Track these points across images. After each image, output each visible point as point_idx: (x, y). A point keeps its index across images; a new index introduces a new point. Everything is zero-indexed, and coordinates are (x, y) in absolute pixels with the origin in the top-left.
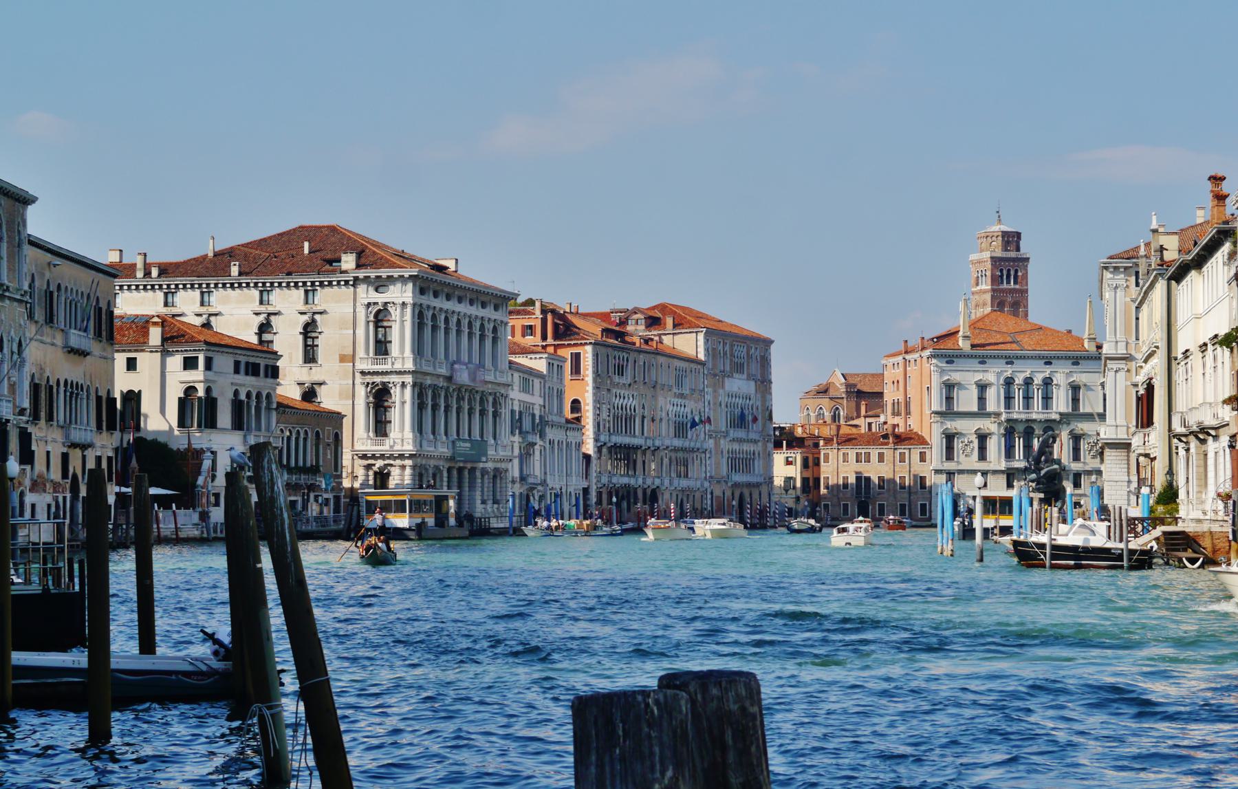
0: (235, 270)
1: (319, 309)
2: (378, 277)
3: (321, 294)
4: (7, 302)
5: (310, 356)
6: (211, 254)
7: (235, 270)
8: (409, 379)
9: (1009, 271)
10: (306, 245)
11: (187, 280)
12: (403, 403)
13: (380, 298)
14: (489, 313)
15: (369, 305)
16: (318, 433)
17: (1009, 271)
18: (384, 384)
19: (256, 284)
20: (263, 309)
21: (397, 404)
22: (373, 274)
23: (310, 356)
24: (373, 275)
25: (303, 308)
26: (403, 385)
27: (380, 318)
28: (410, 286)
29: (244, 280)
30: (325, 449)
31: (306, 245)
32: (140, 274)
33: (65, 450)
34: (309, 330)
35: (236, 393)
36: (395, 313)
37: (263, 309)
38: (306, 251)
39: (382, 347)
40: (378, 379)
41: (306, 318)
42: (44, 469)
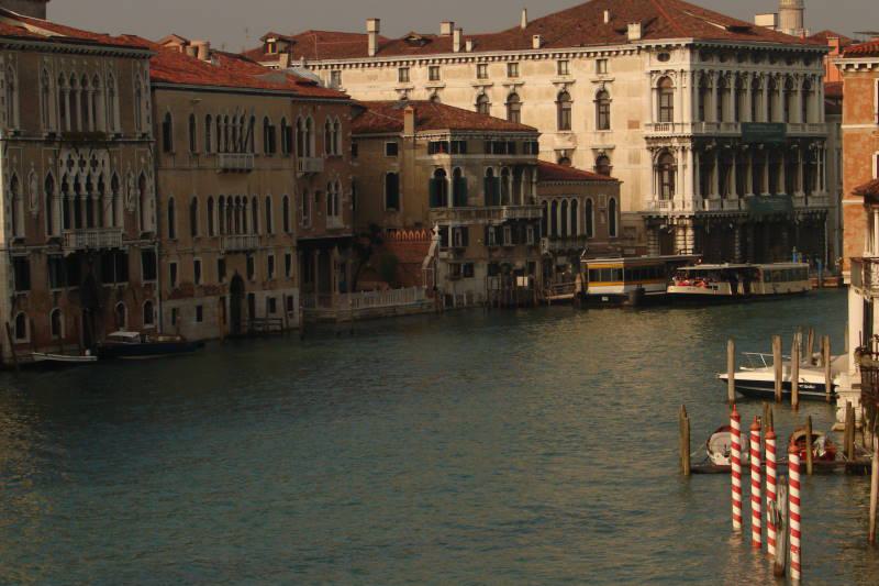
0: (536, 43)
1: (610, 77)
2: (657, 46)
3: (611, 63)
4: (122, 146)
5: (603, 123)
6: (524, 25)
7: (536, 43)
8: (688, 145)
9: (565, 203)
10: (606, 13)
11: (496, 54)
12: (685, 167)
13: (663, 66)
14: (798, 67)
15: (652, 72)
16: (589, 201)
17: (565, 203)
18: (666, 148)
19: (554, 55)
20: (560, 79)
21: (680, 168)
22: (653, 43)
23: (603, 123)
24: (653, 45)
25: (596, 78)
26: (684, 150)
27: (663, 87)
28: (688, 53)
29: (543, 52)
30: (597, 215)
31: (606, 13)
32: (456, 48)
33: (222, 257)
34: (602, 100)
35: (490, 171)
36: (676, 81)
37: (560, 79)
38: (606, 20)
39: (665, 111)
40: (661, 145)
41: (596, 88)
42: (192, 279)
